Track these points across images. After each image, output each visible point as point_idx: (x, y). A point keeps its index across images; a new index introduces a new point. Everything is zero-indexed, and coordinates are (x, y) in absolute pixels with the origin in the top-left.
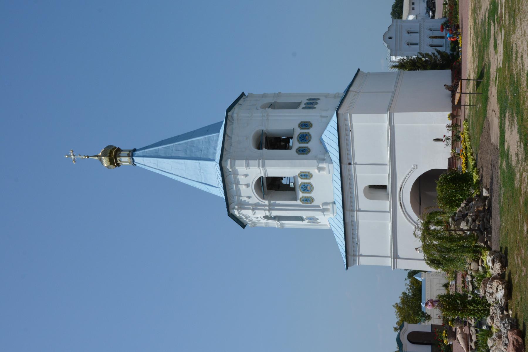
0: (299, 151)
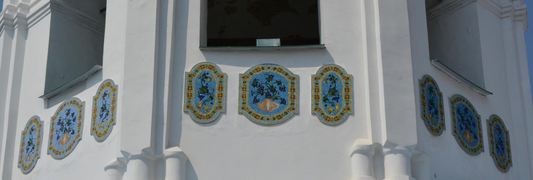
0: (431, 90)
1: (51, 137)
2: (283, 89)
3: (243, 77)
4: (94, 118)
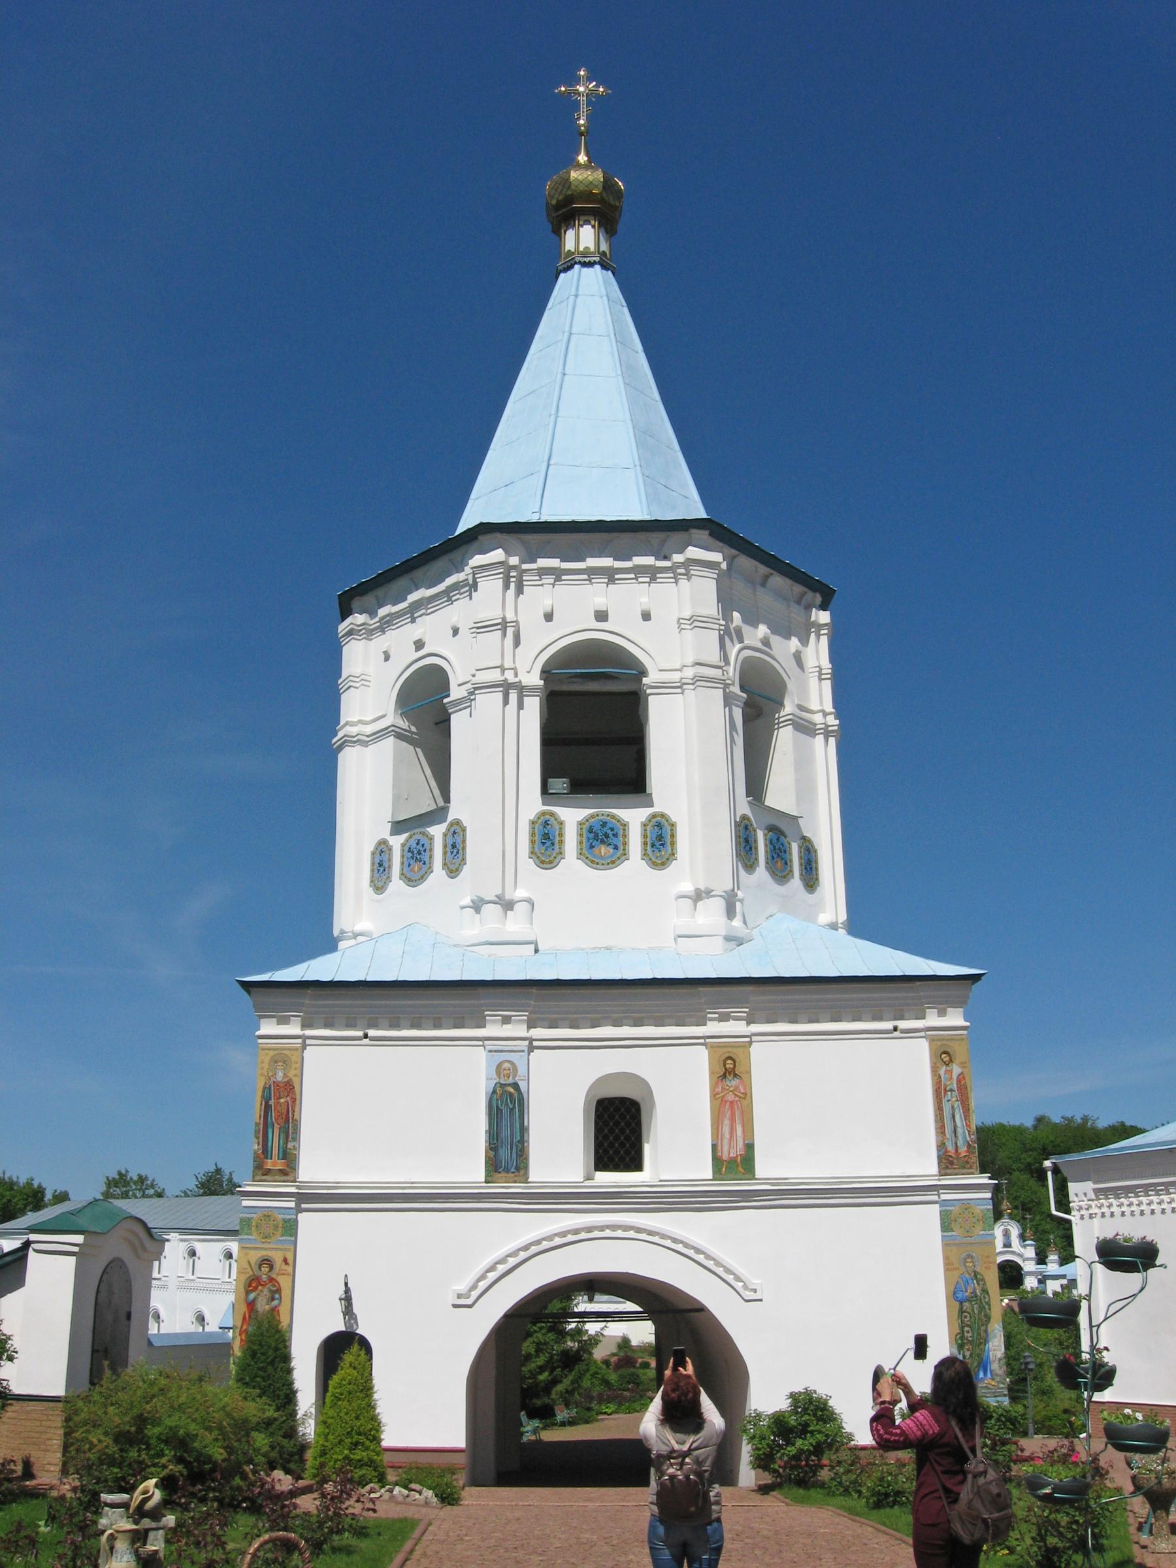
0: (746, 828)
1: (402, 863)
2: (616, 835)
3: (580, 824)
4: (445, 853)
